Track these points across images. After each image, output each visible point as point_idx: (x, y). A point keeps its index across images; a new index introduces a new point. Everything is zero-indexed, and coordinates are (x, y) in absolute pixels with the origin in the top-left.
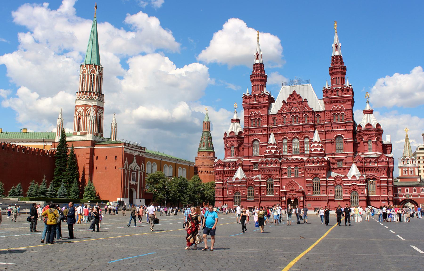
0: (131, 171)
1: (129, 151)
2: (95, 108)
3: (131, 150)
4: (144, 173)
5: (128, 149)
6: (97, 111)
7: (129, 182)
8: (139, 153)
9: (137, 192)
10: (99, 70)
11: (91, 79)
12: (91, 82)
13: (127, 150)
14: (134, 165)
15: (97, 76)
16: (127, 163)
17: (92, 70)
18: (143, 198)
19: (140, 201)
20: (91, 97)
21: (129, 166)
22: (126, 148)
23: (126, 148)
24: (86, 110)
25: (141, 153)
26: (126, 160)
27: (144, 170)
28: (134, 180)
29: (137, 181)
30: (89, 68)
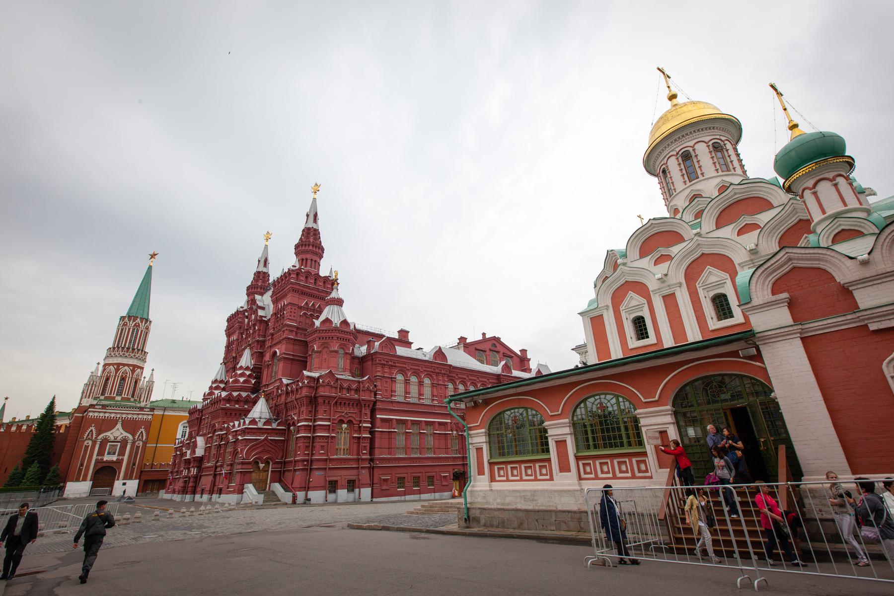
0: (105, 441)
1: (102, 415)
4: (145, 443)
6: (117, 370)
7: (95, 457)
8: (135, 417)
13: (96, 414)
14: (118, 432)
21: (98, 435)
25: (140, 416)
28: (114, 454)
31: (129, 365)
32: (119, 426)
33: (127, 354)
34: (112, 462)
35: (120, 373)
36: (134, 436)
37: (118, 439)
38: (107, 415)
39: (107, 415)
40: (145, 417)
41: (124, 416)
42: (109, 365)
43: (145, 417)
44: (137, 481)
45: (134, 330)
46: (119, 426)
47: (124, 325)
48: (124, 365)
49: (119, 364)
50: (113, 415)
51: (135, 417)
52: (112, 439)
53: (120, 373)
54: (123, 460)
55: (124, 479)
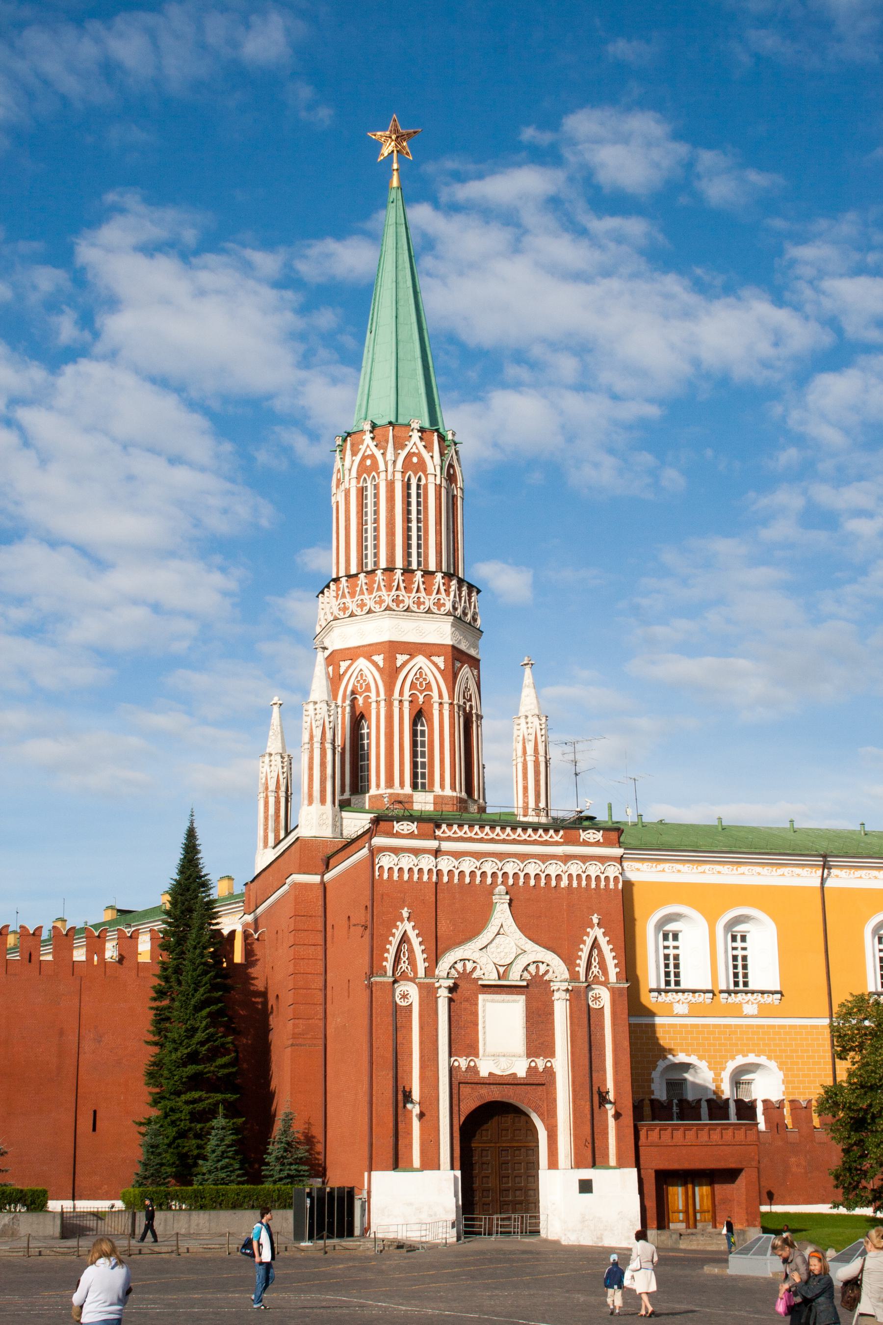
1: (427, 862)
2: (379, 659)
3: (457, 855)
5: (416, 852)
6: (391, 673)
8: (553, 869)
10: (399, 445)
11: (362, 506)
12: (362, 523)
13: (407, 862)
14: (502, 946)
15: (391, 485)
16: (415, 941)
17: (364, 458)
18: (620, 1165)
19: (586, 1186)
20: (362, 605)
21: (434, 958)
22: (396, 851)
23: (396, 851)
24: (340, 677)
25: (575, 868)
26: (408, 926)
27: (613, 972)
30: (354, 453)
31: (428, 650)
32: (502, 914)
33: (408, 600)
34: (512, 1082)
35: (403, 691)
36: (570, 962)
37: (514, 977)
38: (445, 864)
39: (445, 864)
40: (594, 870)
41: (511, 868)
42: (352, 654)
43: (594, 870)
44: (632, 1174)
45: (407, 486)
46: (502, 914)
47: (363, 470)
48: (413, 649)
49: (393, 648)
50: (468, 865)
51: (553, 869)
52: (491, 978)
53: (403, 691)
54: (550, 1072)
55: (578, 1164)
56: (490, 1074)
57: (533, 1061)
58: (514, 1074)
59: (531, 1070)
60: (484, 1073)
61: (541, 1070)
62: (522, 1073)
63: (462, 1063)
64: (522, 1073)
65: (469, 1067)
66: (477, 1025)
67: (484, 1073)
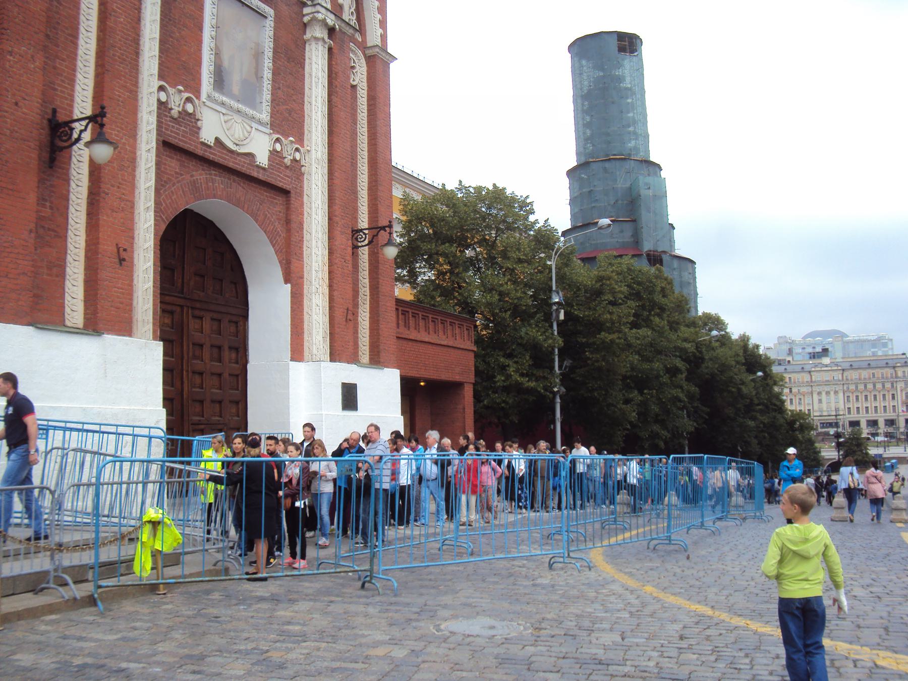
9: (292, 274)
18: (376, 360)
19: (349, 397)
29: (287, 119)
54: (296, 169)
55: (341, 350)
56: (217, 140)
57: (278, 140)
58: (251, 156)
59: (275, 155)
60: (208, 134)
61: (287, 161)
62: (263, 159)
63: (176, 100)
64: (263, 159)
65: (184, 113)
66: (201, 29)
67: (208, 134)
